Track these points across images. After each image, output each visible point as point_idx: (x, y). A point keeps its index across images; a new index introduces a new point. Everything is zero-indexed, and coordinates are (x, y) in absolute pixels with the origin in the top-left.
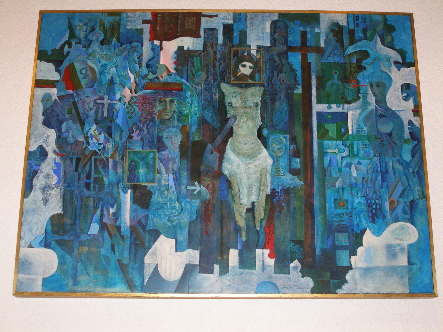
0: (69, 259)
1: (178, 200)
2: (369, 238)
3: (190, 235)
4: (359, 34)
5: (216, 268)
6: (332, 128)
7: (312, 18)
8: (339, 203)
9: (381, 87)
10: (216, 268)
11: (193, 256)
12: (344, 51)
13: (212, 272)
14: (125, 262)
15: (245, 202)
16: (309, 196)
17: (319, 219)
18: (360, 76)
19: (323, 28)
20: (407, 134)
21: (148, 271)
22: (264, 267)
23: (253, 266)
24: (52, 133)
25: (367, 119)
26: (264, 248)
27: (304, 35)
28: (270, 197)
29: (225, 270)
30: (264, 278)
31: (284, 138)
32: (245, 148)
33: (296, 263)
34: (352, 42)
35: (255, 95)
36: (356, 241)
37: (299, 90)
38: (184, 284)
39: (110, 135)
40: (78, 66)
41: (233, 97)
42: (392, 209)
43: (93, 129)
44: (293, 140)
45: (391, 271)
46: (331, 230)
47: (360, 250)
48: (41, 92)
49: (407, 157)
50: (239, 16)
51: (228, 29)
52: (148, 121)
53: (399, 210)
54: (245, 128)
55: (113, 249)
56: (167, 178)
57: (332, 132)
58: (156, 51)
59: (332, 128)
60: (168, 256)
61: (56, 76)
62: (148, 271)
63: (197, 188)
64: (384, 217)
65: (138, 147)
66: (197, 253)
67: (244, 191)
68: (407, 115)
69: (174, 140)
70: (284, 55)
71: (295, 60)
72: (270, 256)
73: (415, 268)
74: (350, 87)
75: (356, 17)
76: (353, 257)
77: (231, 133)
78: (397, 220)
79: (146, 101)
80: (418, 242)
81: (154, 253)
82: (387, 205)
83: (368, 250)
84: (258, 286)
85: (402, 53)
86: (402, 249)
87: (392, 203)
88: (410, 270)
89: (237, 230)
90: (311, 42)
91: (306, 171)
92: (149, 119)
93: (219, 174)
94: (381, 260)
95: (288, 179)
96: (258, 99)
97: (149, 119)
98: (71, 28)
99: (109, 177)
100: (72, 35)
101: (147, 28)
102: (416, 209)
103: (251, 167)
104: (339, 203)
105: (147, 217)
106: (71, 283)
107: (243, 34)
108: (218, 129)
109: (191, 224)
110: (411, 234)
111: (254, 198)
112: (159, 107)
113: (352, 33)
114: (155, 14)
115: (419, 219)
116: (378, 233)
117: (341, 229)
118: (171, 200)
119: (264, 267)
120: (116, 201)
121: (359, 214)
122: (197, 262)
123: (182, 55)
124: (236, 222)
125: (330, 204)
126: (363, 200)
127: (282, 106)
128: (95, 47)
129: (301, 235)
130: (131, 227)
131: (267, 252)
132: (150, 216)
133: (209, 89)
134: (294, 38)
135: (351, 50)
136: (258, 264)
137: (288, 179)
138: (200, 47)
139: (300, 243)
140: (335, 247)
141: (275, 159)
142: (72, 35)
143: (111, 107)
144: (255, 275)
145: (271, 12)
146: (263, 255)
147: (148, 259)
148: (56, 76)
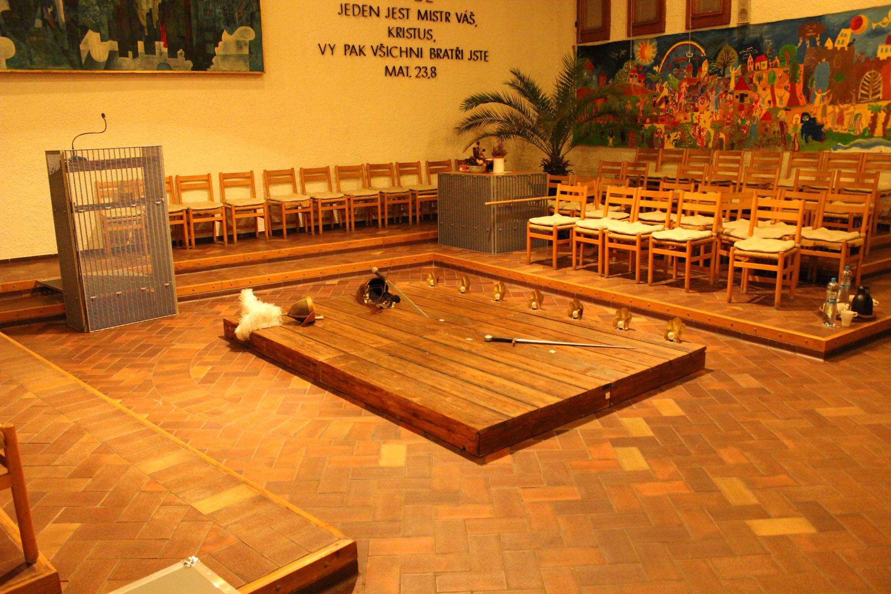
0: (23, 46)
1: (98, 4)
2: (225, 36)
3: (109, 29)
5: (130, 53)
10: (130, 53)
11: (114, 45)
13: (127, 56)
14: (66, 47)
17: (194, 22)
21: (84, 56)
22: (161, 54)
23: (154, 53)
26: (160, 40)
29: (136, 55)
30: (162, 61)
33: (180, 51)
42: (240, 18)
45: (240, 57)
47: (220, 43)
53: (244, 19)
55: (56, 39)
60: (96, 46)
64: (235, 23)
66: (115, 44)
72: (165, 46)
73: (253, 56)
76: (216, 49)
78: (242, 25)
80: (256, 38)
81: (86, 43)
82: (236, 14)
83: (225, 44)
84: (159, 66)
86: (246, 44)
87: (239, 13)
88: (250, 57)
89: (142, 27)
94: (233, 51)
102: (254, 19)
105: (77, 16)
106: (28, 63)
109: (109, 22)
110: (251, 35)
111: (151, 6)
116: (231, 32)
118: (92, 4)
119: (161, 54)
121: (219, 19)
122: (117, 49)
124: (140, 23)
125: (201, 13)
126: (221, 11)
130: (67, 24)
131: (162, 43)
132: (80, 16)
136: (157, 51)
139: (183, 38)
144: (156, 59)
146: (160, 45)
147: (82, 47)
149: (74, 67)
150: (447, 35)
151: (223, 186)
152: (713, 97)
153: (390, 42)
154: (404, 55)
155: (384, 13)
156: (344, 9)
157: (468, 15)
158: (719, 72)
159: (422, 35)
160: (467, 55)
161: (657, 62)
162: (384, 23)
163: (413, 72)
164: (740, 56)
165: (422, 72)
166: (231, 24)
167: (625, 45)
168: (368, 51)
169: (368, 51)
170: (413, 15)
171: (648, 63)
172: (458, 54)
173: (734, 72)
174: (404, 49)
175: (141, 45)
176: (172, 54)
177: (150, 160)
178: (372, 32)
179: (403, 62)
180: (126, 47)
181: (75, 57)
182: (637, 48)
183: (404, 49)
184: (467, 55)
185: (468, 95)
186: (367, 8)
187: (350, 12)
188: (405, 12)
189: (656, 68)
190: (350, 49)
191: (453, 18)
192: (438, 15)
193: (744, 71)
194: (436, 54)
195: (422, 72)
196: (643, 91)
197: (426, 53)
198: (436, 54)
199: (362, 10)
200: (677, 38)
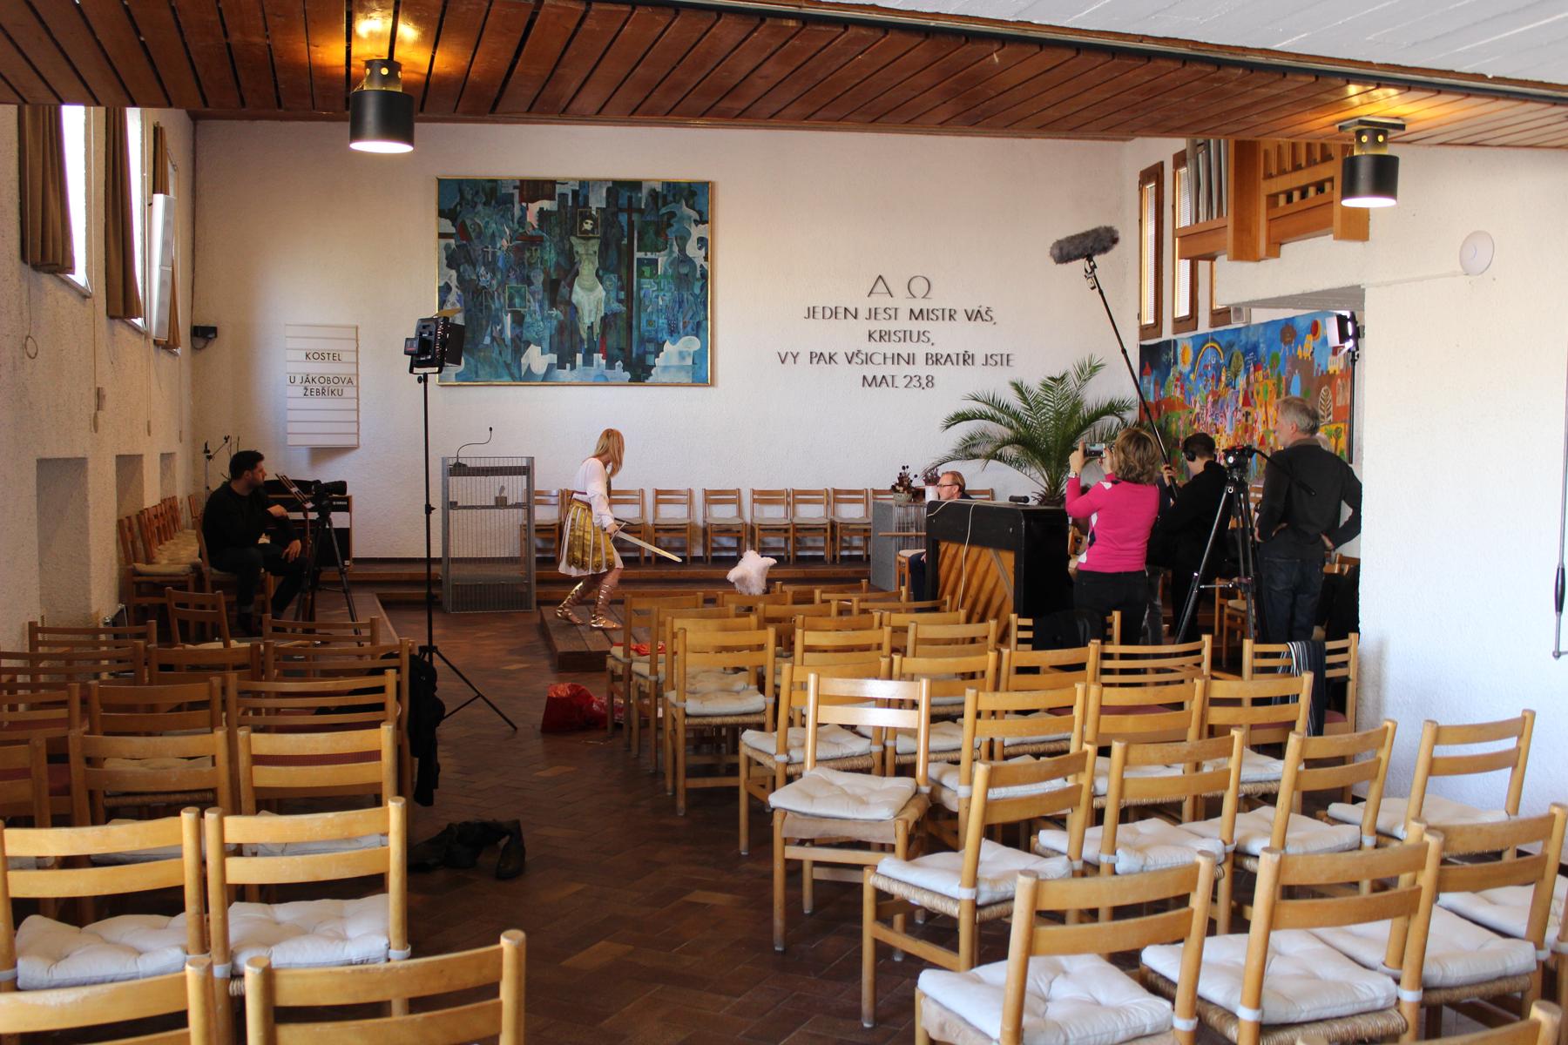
2: (668, 346)
4: (670, 198)
6: (647, 270)
7: (636, 185)
8: (650, 322)
9: (683, 239)
11: (553, 358)
12: (658, 210)
15: (587, 321)
16: (630, 318)
17: (635, 333)
18: (669, 231)
19: (645, 191)
20: (698, 275)
21: (524, 369)
24: (454, 273)
25: (671, 263)
27: (630, 198)
28: (603, 319)
29: (573, 367)
31: (614, 277)
32: (587, 284)
34: (665, 204)
35: (594, 246)
36: (659, 348)
37: (625, 242)
38: (547, 378)
39: (494, 274)
40: (468, 223)
41: (580, 247)
43: (482, 270)
44: (620, 278)
45: (681, 368)
46: (642, 341)
48: (444, 242)
49: (697, 291)
50: (584, 184)
51: (575, 193)
52: (521, 267)
54: (588, 269)
56: (533, 306)
57: (647, 273)
58: (524, 211)
59: (647, 270)
60: (537, 359)
61: (453, 230)
62: (524, 369)
63: (555, 312)
65: (514, 284)
67: (586, 313)
68: (699, 261)
69: (539, 279)
70: (615, 214)
71: (623, 218)
74: (661, 240)
75: (669, 185)
77: (577, 274)
79: (519, 250)
85: (700, 213)
89: (582, 341)
90: (635, 205)
91: (629, 300)
92: (520, 263)
93: (569, 303)
94: (675, 361)
95: (616, 306)
96: (596, 248)
97: (520, 263)
98: (461, 191)
99: (495, 305)
100: (462, 197)
101: (516, 192)
103: (591, 298)
104: (650, 322)
107: (586, 198)
108: (569, 270)
112: (527, 254)
113: (665, 197)
114: (522, 181)
115: (702, 334)
116: (674, 343)
117: (650, 340)
120: (500, 321)
123: (542, 213)
125: (644, 323)
127: (613, 254)
128: (480, 207)
129: (623, 344)
130: (513, 340)
133: (562, 240)
134: (623, 202)
135: (663, 211)
137: (616, 306)
138: (555, 208)
139: (622, 349)
140: (646, 353)
141: (608, 292)
142: (462, 197)
143: (494, 254)
144: (593, 371)
145: (607, 181)
146: (598, 358)
147: (523, 360)
148: (453, 230)
149: (513, 378)
150: (946, 337)
151: (658, 502)
152: (1228, 414)
153: (869, 347)
154: (889, 361)
155: (863, 313)
156: (811, 313)
157: (983, 311)
158: (1230, 384)
159: (915, 338)
160: (980, 359)
161: (1192, 371)
162: (864, 325)
163: (901, 382)
164: (1246, 363)
165: (915, 382)
166: (673, 331)
167: (1169, 345)
168: (841, 358)
169: (841, 358)
170: (904, 314)
171: (1186, 369)
172: (967, 359)
173: (1241, 382)
174: (889, 355)
175: (579, 357)
176: (610, 366)
177: (526, 471)
178: (847, 336)
179: (889, 370)
180: (565, 360)
181: (515, 371)
182: (1179, 350)
183: (889, 355)
184: (980, 359)
185: (952, 414)
186: (841, 311)
187: (819, 315)
188: (892, 313)
189: (1192, 377)
190: (817, 357)
191: (961, 316)
192: (939, 314)
193: (1248, 383)
194: (935, 360)
195: (915, 382)
196: (1184, 407)
197: (921, 359)
198: (935, 360)
199: (834, 313)
200: (1205, 338)
